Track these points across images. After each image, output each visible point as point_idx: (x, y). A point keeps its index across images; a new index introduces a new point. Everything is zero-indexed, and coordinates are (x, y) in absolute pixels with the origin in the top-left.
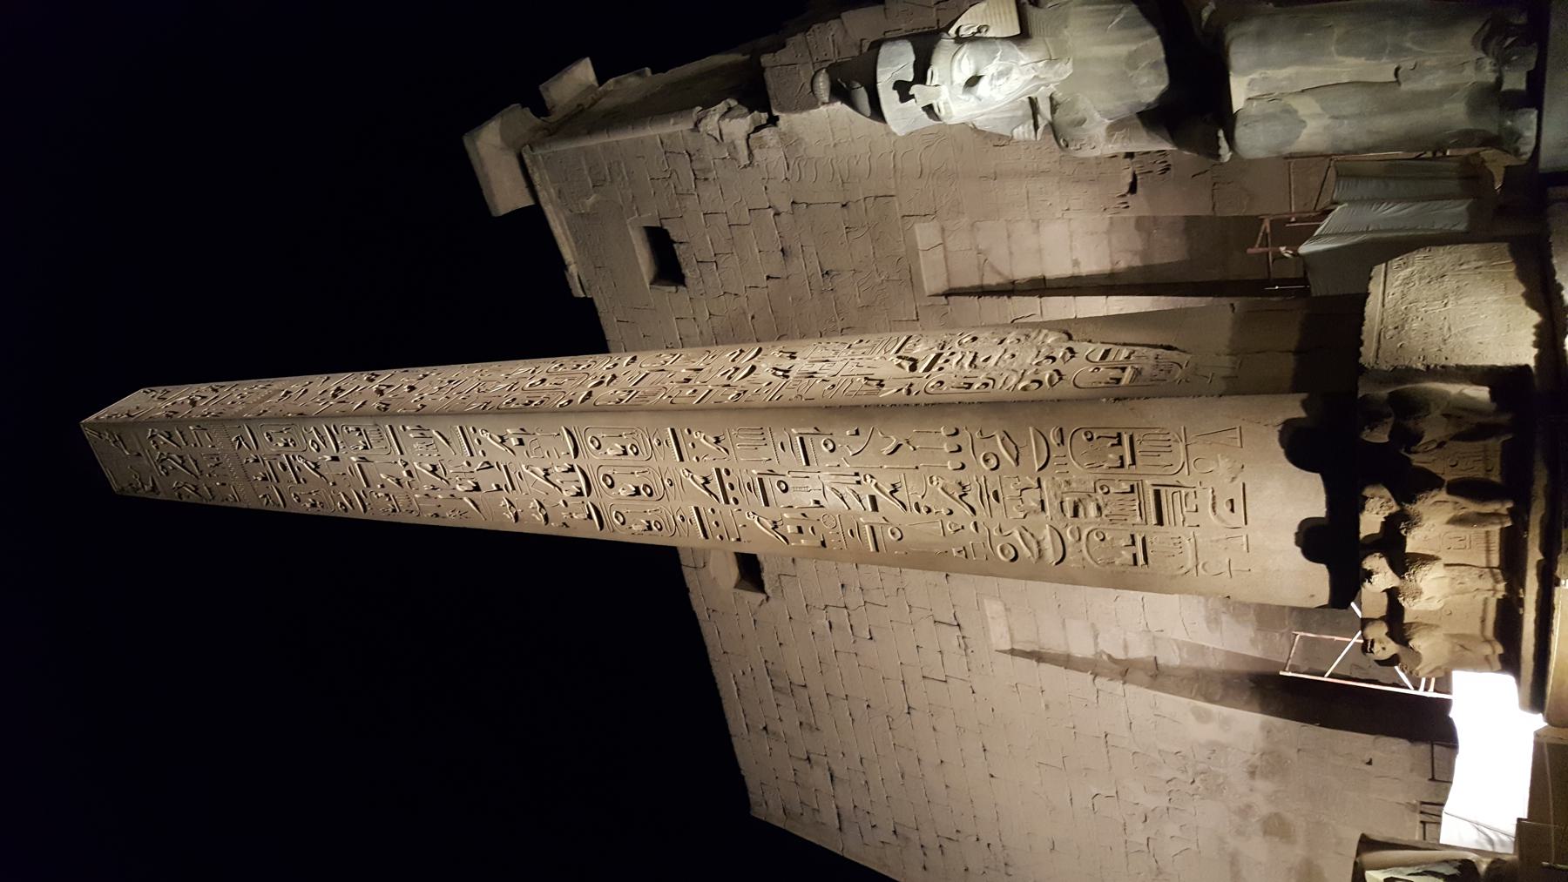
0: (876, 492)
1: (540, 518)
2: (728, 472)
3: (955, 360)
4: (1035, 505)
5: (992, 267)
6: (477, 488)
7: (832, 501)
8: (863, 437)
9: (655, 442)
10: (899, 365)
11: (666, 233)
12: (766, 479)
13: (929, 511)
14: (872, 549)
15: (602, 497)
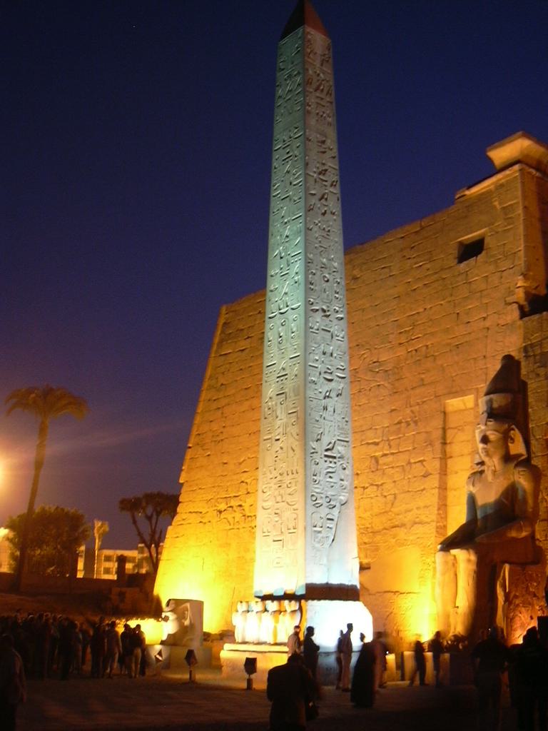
0: (281, 441)
1: (272, 288)
2: (286, 379)
3: (331, 465)
4: (278, 500)
5: (456, 433)
6: (281, 258)
7: (278, 423)
8: (297, 437)
9: (295, 347)
10: (330, 443)
11: (480, 252)
12: (284, 395)
13: (276, 461)
14: (265, 438)
15: (278, 321)
